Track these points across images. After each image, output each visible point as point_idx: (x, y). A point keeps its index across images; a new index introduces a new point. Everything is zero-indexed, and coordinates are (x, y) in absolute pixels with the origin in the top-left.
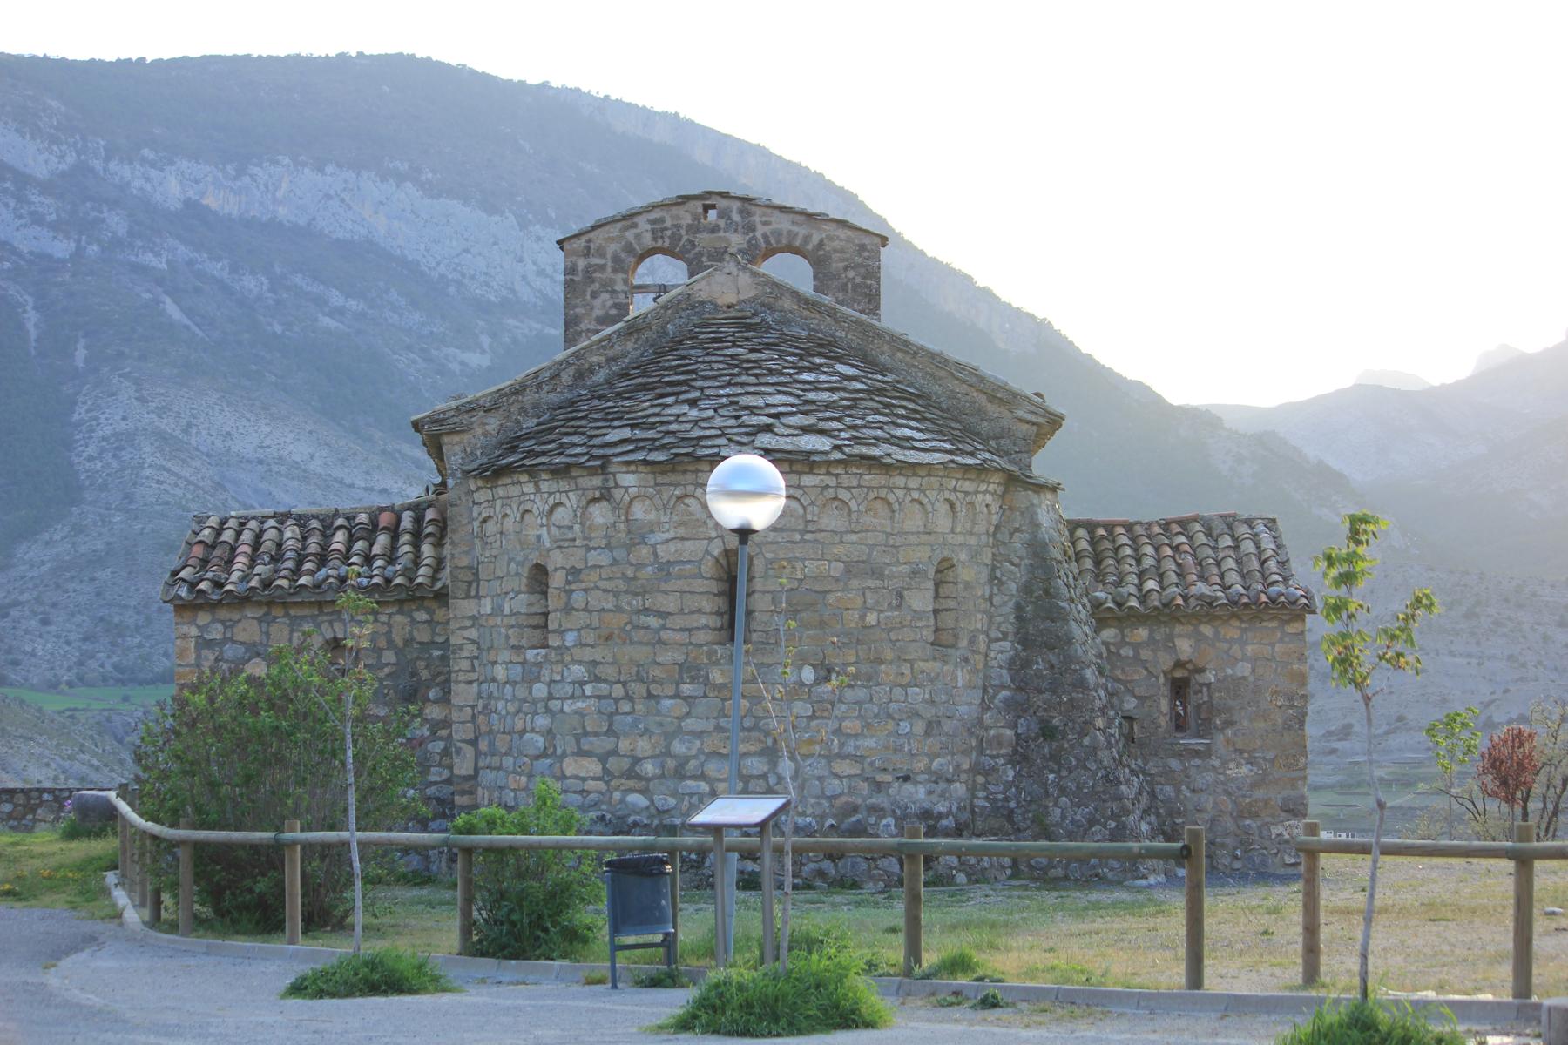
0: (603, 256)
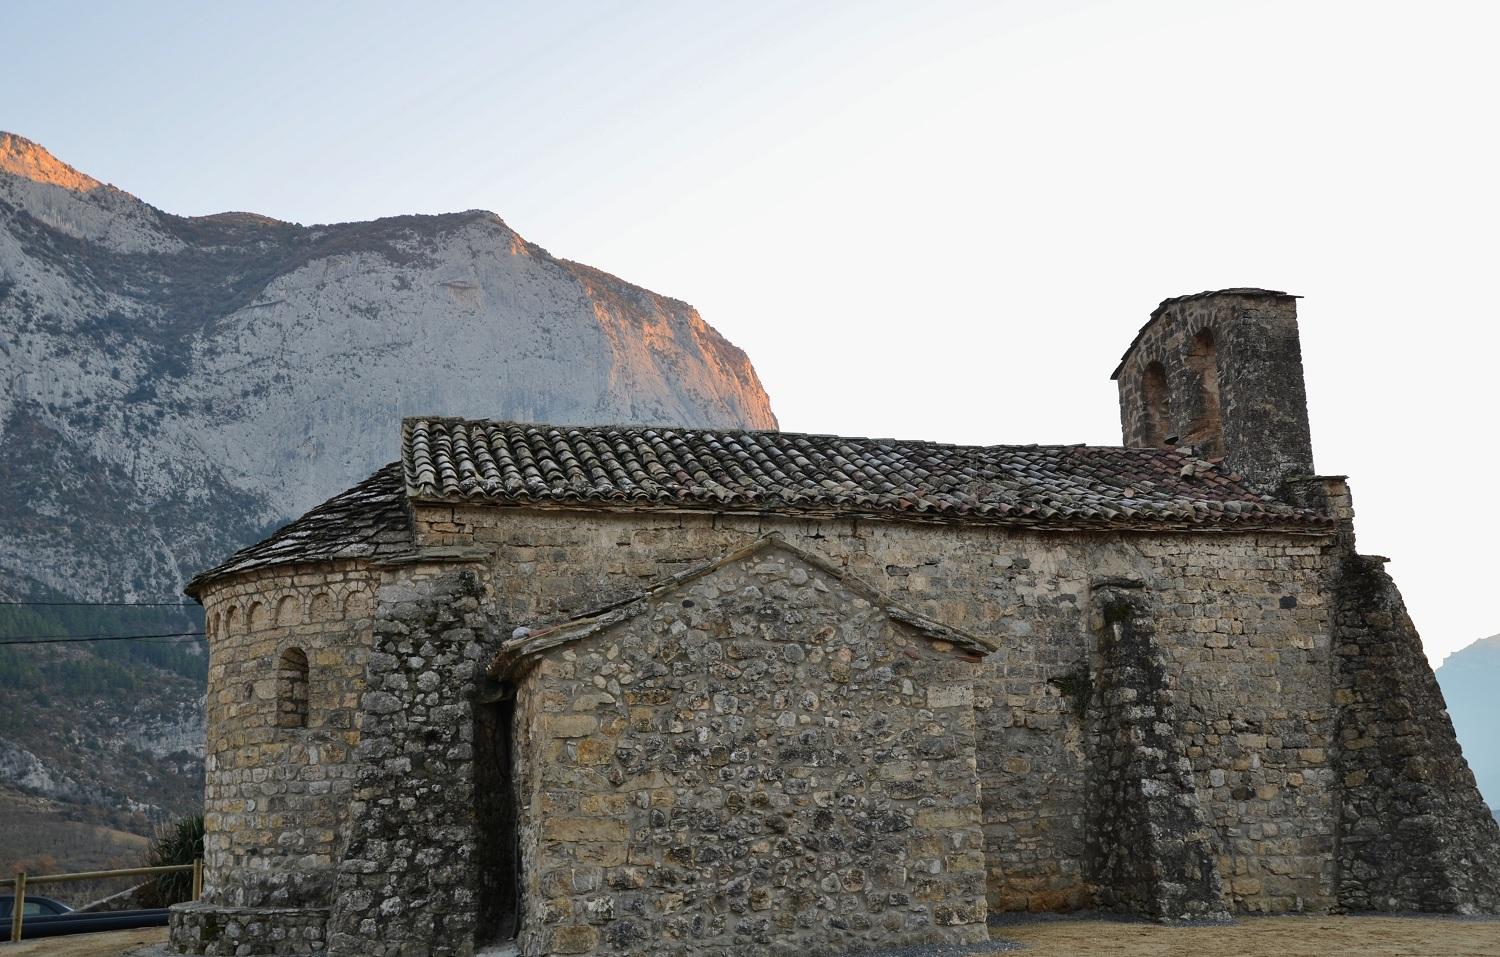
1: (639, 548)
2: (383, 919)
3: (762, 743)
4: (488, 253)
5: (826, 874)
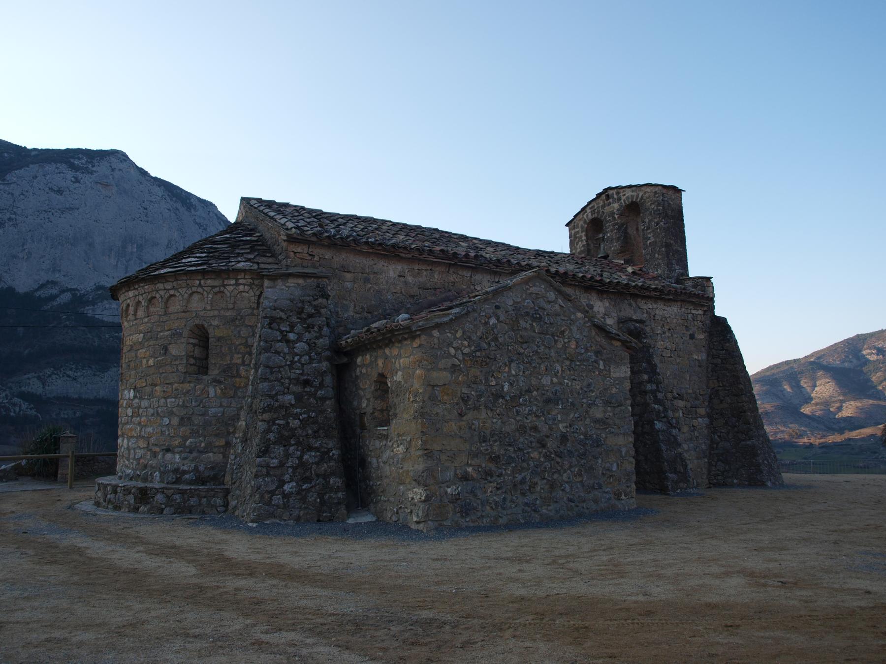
0: (578, 228)
1: (410, 279)
2: (286, 496)
3: (535, 393)
4: (120, 170)
5: (565, 472)
